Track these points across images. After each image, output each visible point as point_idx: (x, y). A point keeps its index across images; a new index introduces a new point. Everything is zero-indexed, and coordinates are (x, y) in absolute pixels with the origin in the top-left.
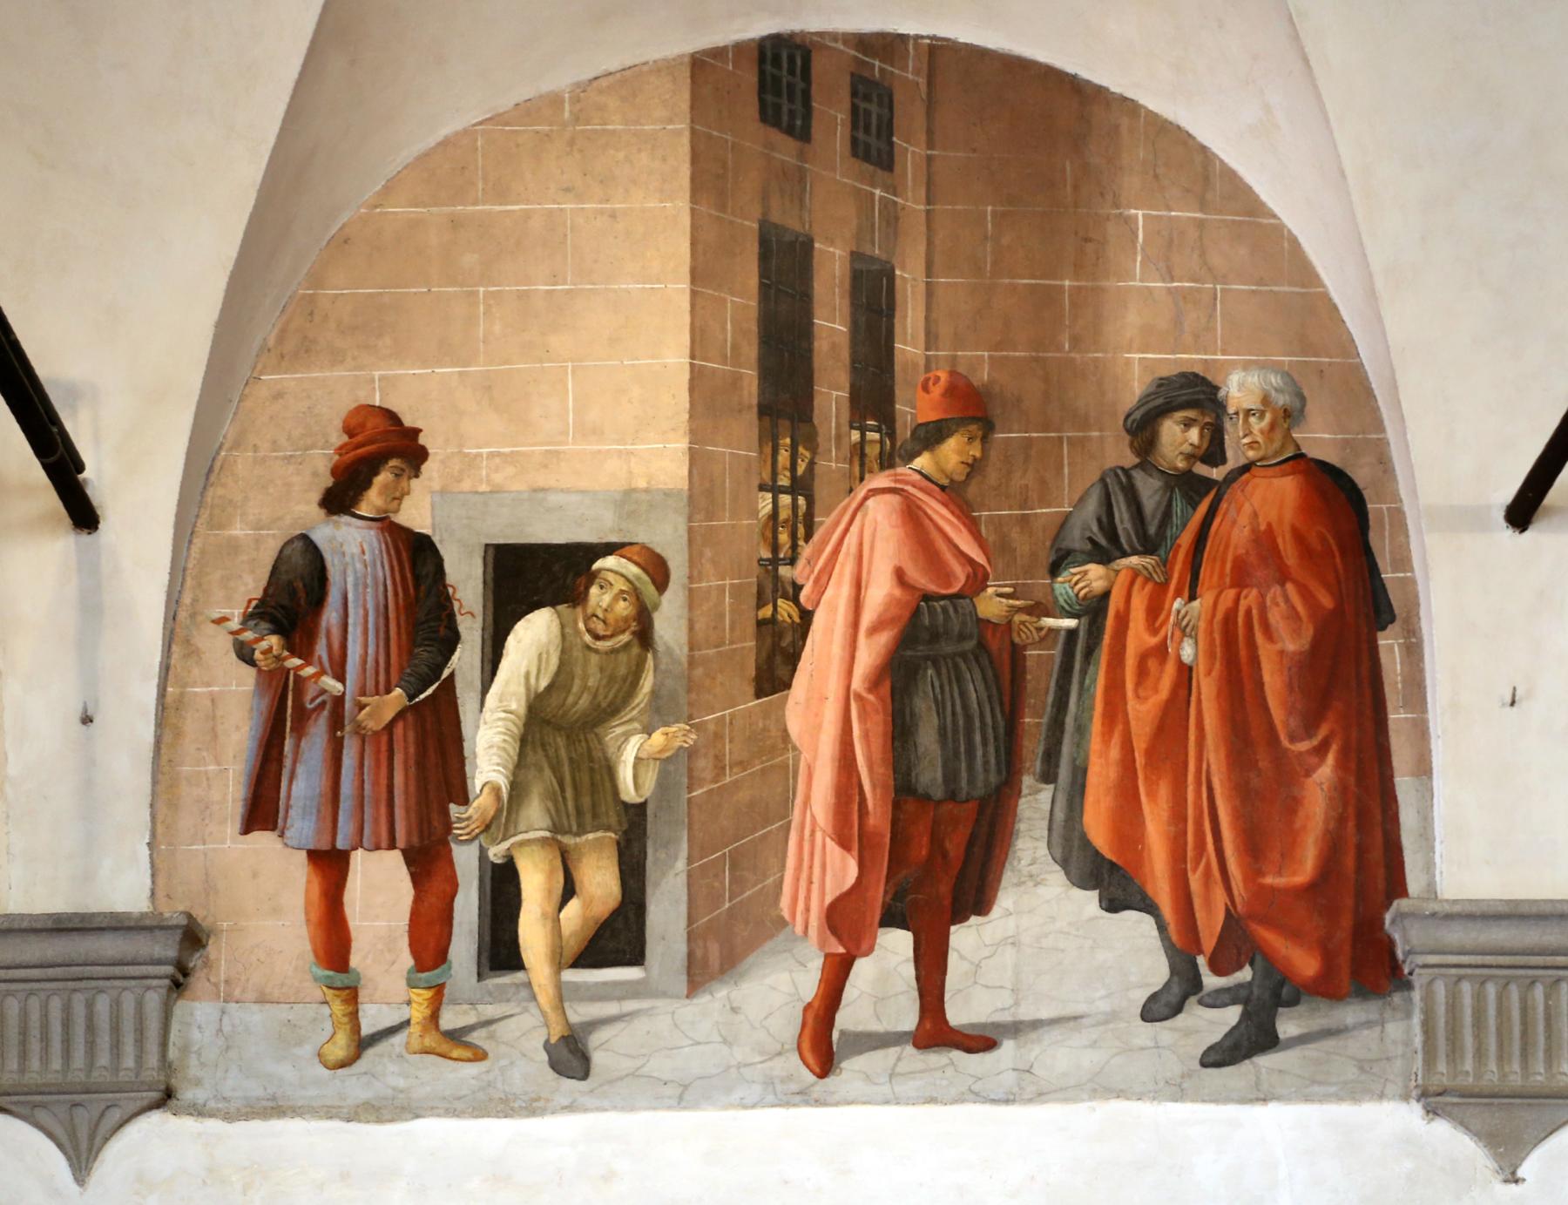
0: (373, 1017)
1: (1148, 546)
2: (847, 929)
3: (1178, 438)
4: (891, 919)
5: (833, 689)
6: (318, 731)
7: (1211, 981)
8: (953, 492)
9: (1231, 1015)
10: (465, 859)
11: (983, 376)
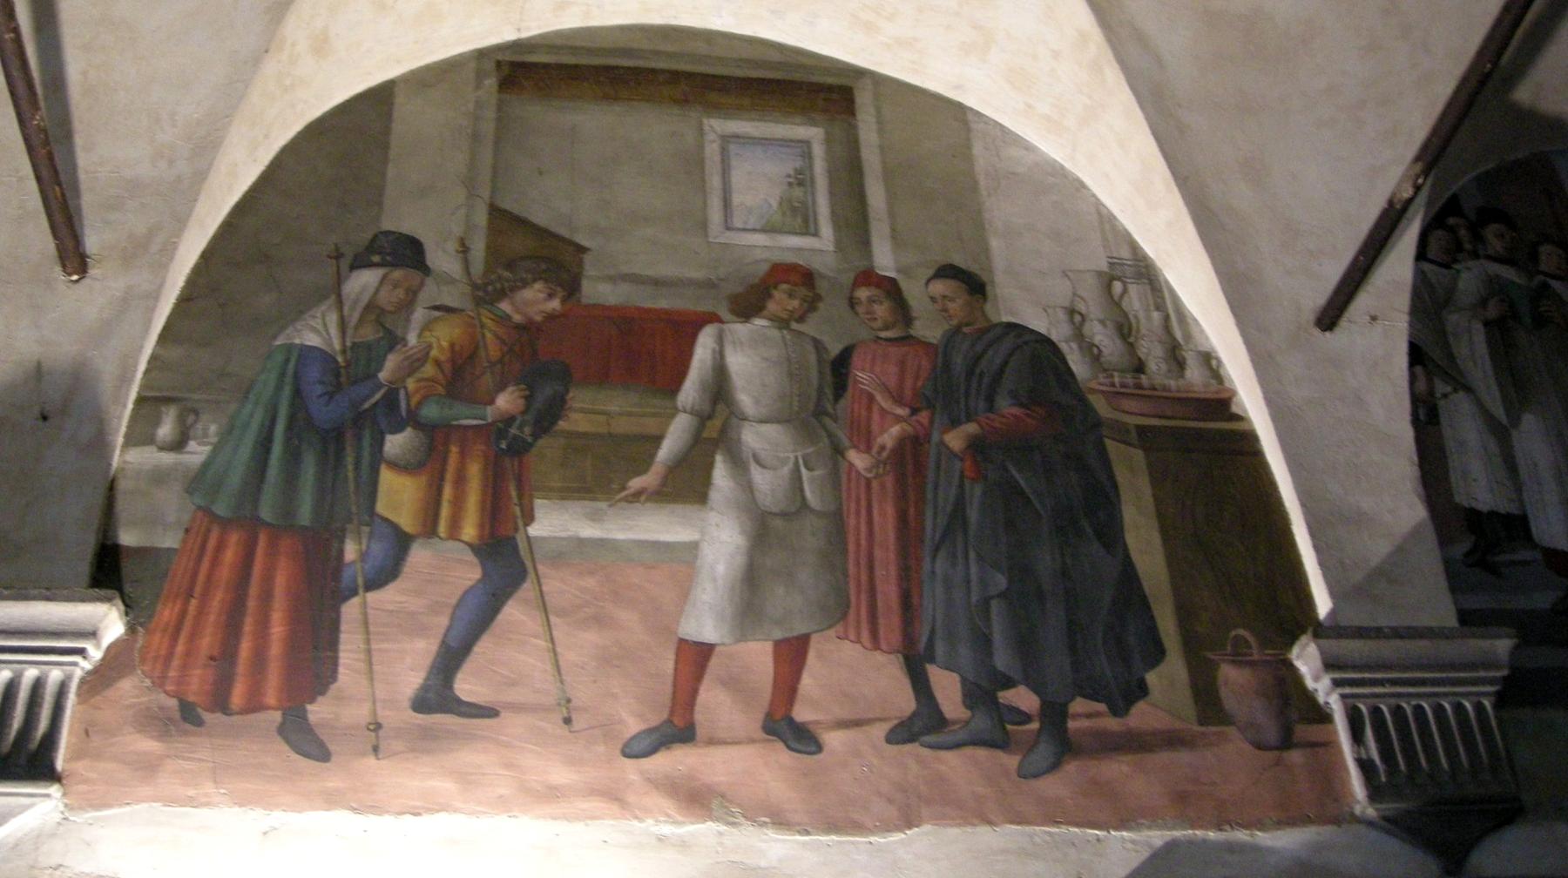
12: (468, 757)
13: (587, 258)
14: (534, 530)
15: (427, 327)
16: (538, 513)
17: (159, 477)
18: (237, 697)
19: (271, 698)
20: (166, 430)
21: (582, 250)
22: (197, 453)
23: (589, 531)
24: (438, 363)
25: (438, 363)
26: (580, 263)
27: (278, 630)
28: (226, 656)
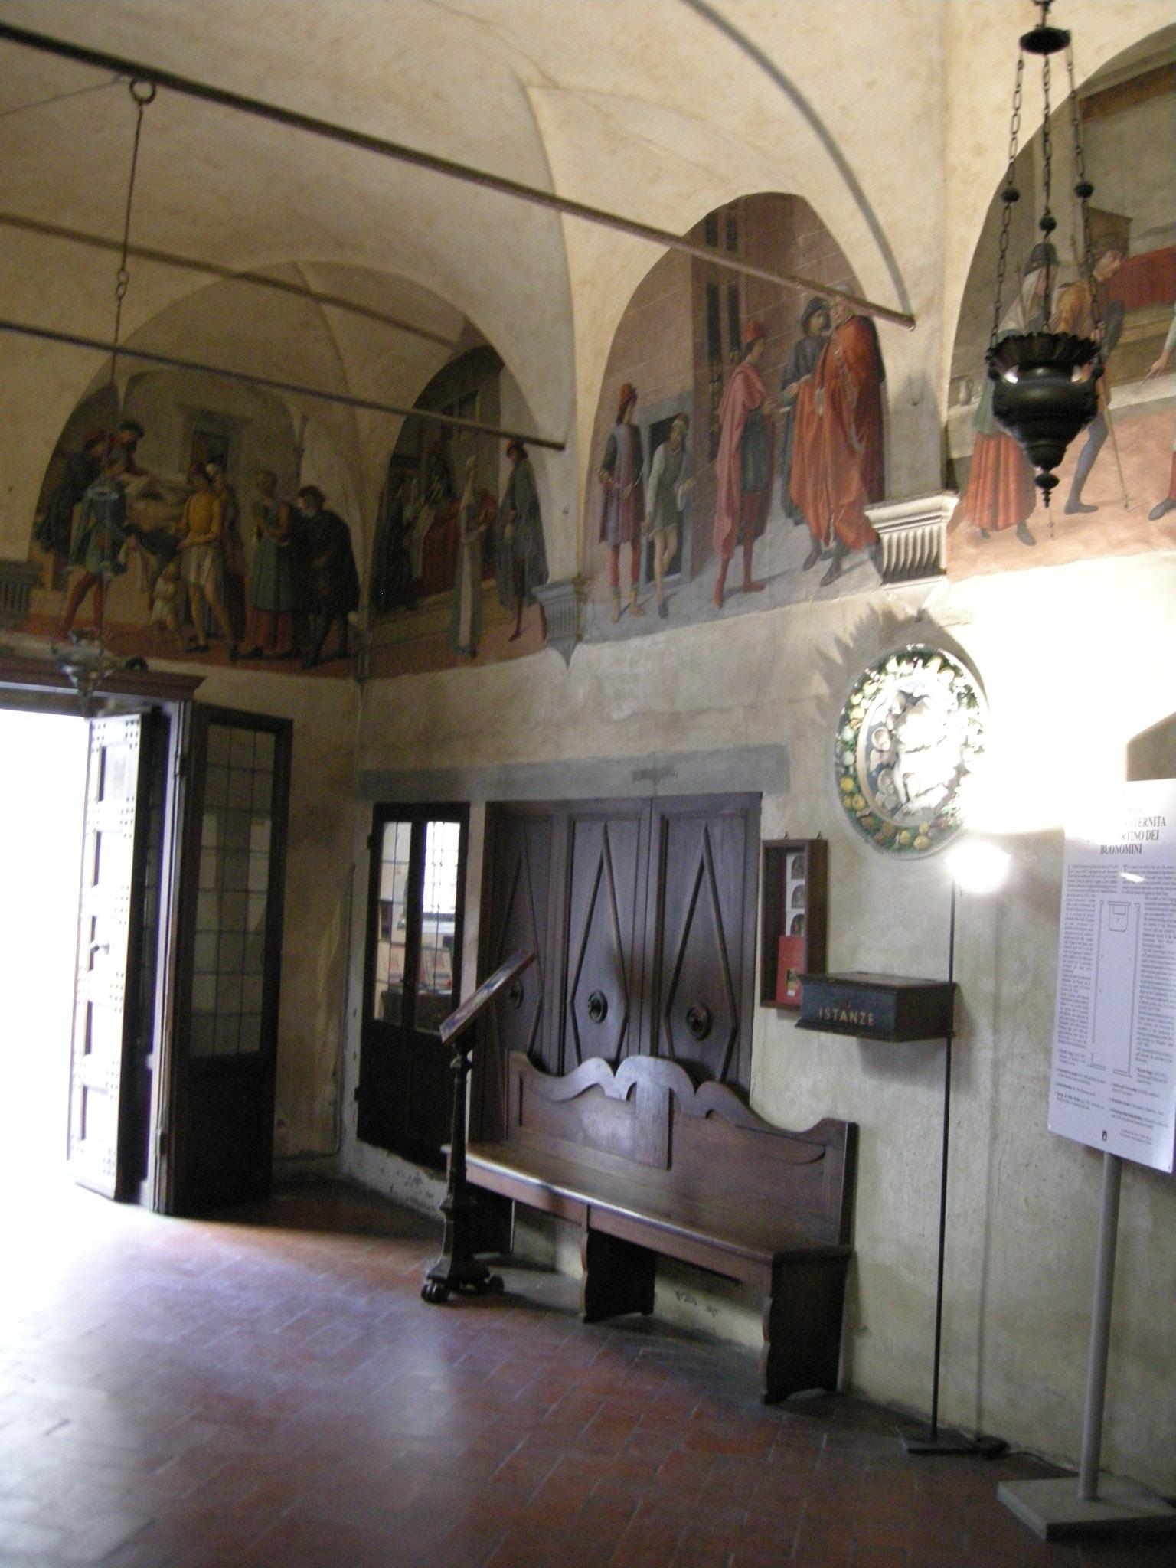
0: (624, 603)
1: (808, 370)
2: (728, 548)
3: (816, 322)
4: (739, 543)
5: (727, 453)
6: (615, 502)
7: (824, 549)
8: (757, 368)
9: (829, 562)
10: (644, 541)
11: (762, 318)
12: (1085, 533)
13: (1132, 225)
14: (1112, 406)
15: (1060, 299)
16: (1113, 395)
17: (962, 419)
18: (1000, 523)
19: (1012, 519)
20: (962, 395)
21: (1128, 220)
22: (976, 402)
23: (1134, 400)
24: (1066, 320)
25: (1066, 320)
26: (1127, 231)
27: (1012, 486)
28: (994, 504)
